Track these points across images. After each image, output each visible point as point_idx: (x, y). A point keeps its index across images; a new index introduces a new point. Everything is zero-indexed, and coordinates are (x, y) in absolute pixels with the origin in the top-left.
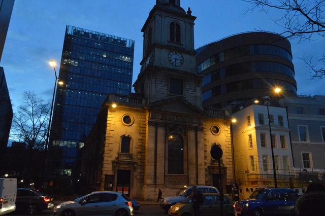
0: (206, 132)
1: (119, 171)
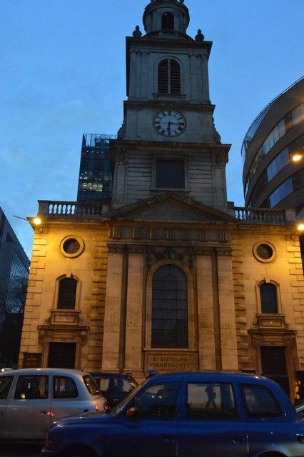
0: (241, 259)
1: (52, 345)
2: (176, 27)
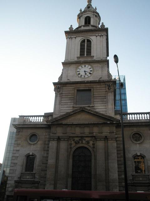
2: (92, 23)
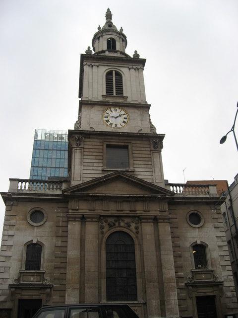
2: (118, 47)
